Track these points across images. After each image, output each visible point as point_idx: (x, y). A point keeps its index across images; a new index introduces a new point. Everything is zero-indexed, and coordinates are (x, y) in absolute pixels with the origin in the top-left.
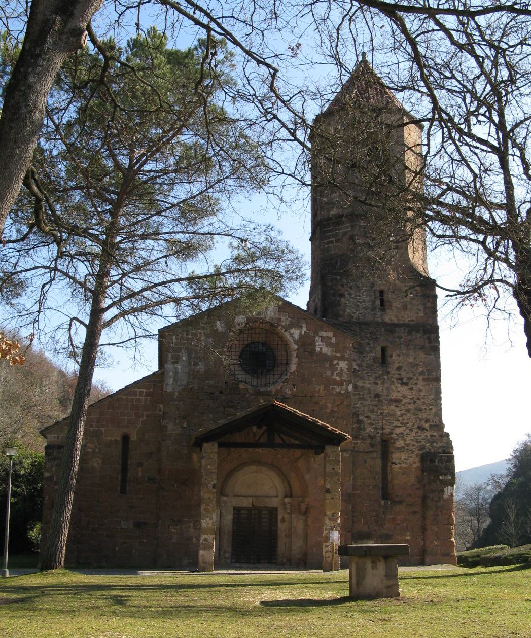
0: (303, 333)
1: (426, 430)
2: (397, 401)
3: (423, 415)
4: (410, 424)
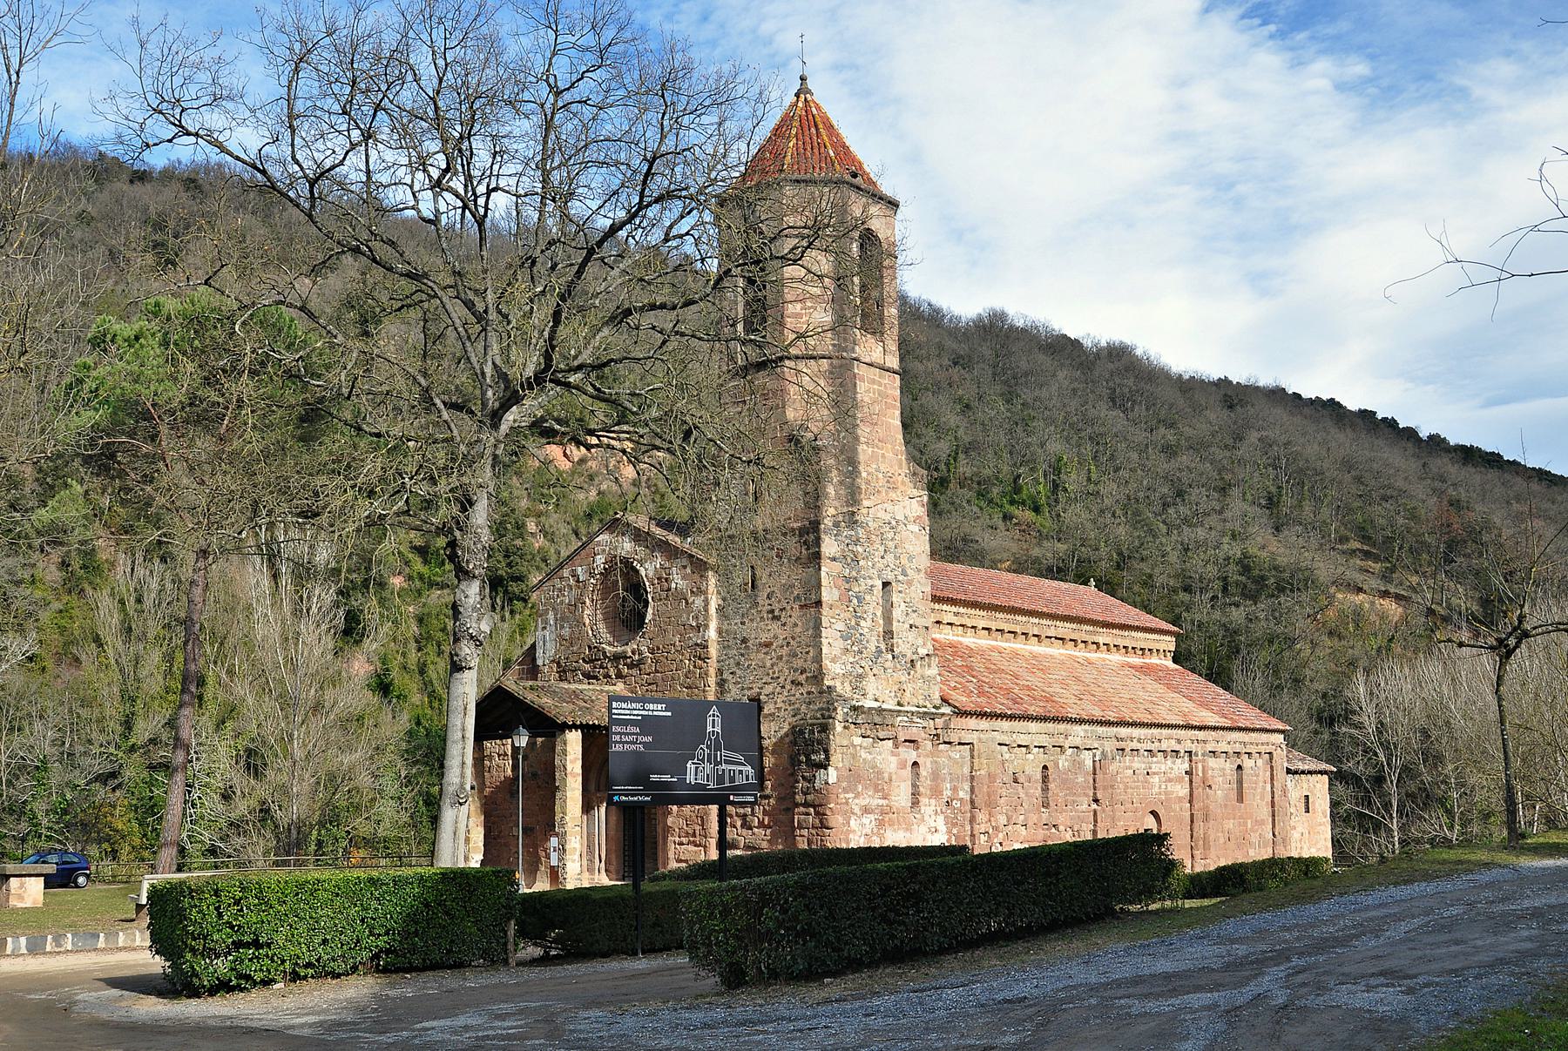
0: (658, 566)
1: (802, 685)
2: (768, 645)
3: (799, 663)
4: (781, 680)
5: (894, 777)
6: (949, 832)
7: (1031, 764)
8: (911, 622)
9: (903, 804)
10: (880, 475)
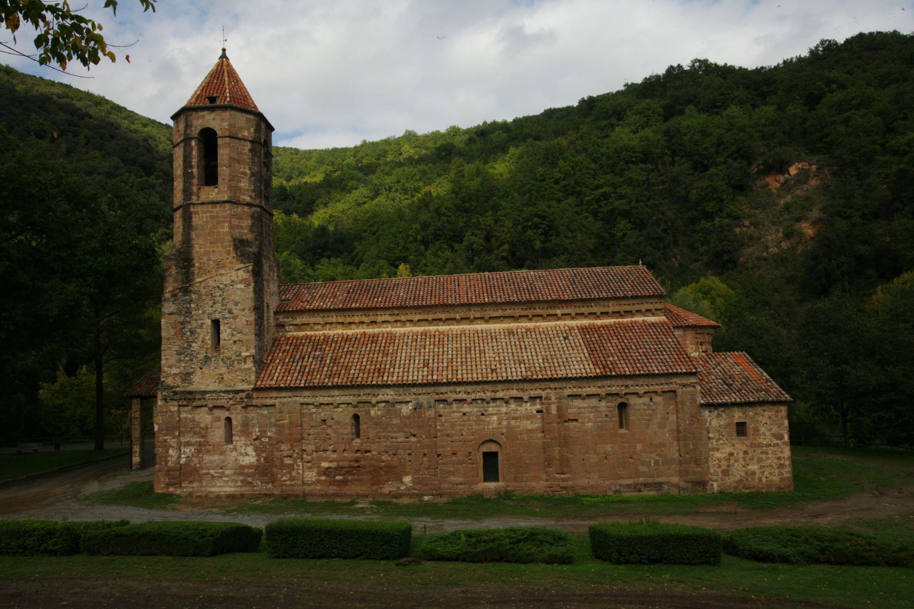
5: (209, 426)
6: (258, 455)
7: (343, 415)
8: (236, 339)
9: (217, 440)
10: (211, 262)
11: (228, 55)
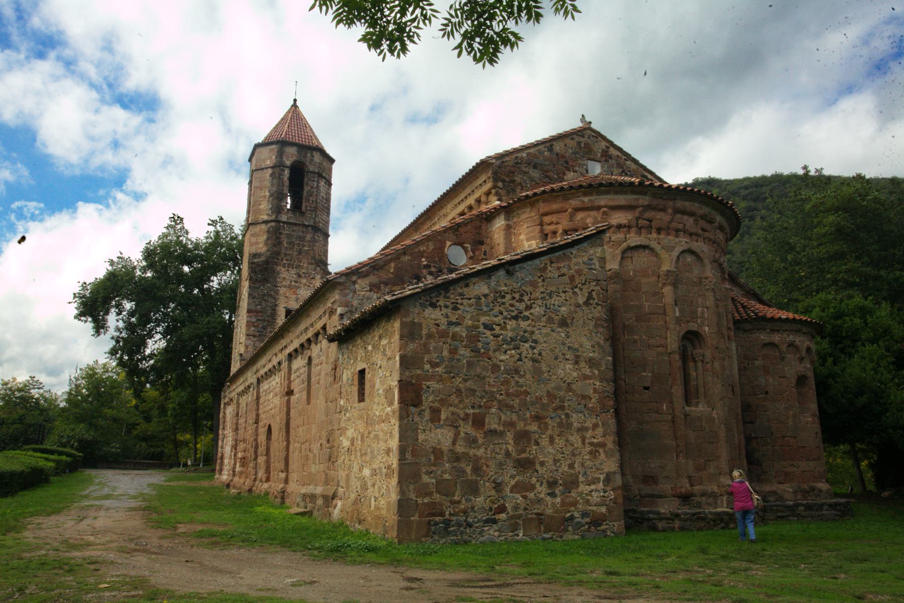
11: (298, 103)
